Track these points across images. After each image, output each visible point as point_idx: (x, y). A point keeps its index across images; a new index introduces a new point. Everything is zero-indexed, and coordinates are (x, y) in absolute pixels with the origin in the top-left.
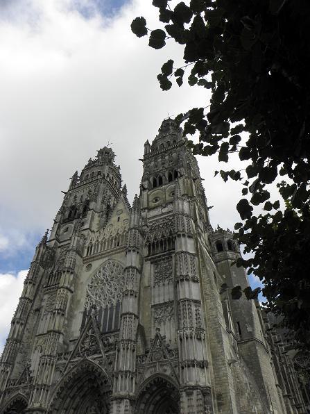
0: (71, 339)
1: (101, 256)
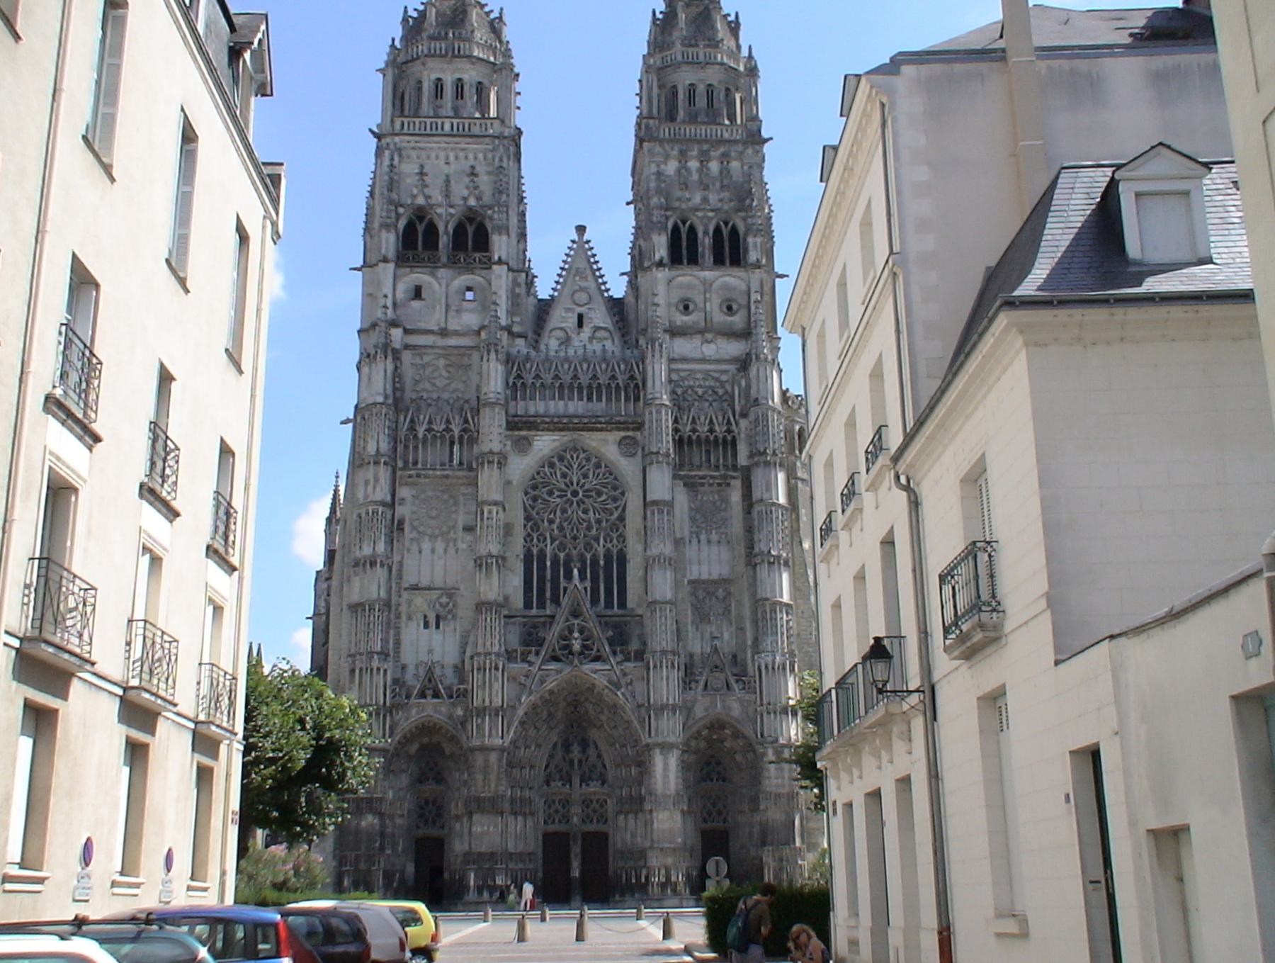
0: (506, 613)
1: (556, 424)
